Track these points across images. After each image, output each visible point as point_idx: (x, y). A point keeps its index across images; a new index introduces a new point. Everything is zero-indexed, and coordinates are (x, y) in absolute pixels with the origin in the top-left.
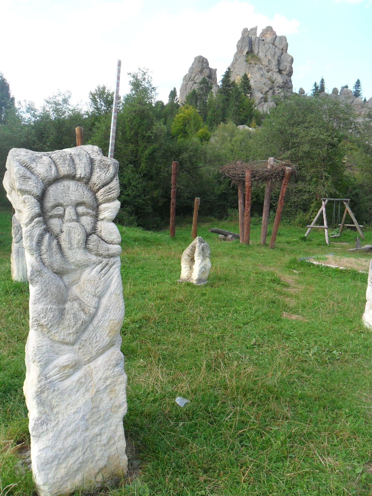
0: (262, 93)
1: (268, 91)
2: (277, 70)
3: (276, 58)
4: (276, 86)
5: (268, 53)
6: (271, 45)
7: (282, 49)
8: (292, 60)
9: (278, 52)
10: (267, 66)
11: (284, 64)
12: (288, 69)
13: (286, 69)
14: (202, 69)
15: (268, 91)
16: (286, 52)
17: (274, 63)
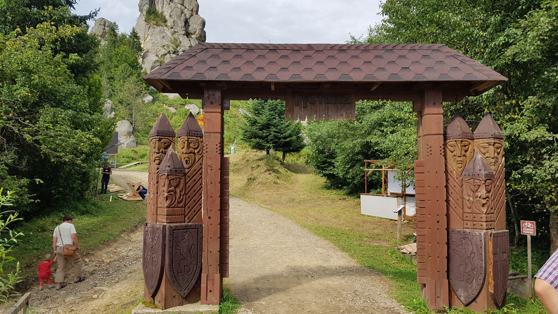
0: (157, 56)
1: (166, 54)
2: (184, 32)
3: (183, 18)
4: (181, 50)
5: (174, 13)
6: (179, 6)
7: (192, 11)
8: (204, 24)
9: (187, 13)
10: (172, 28)
11: (194, 26)
12: (197, 32)
13: (195, 32)
14: (103, 33)
15: (166, 54)
16: (197, 14)
17: (181, 23)
